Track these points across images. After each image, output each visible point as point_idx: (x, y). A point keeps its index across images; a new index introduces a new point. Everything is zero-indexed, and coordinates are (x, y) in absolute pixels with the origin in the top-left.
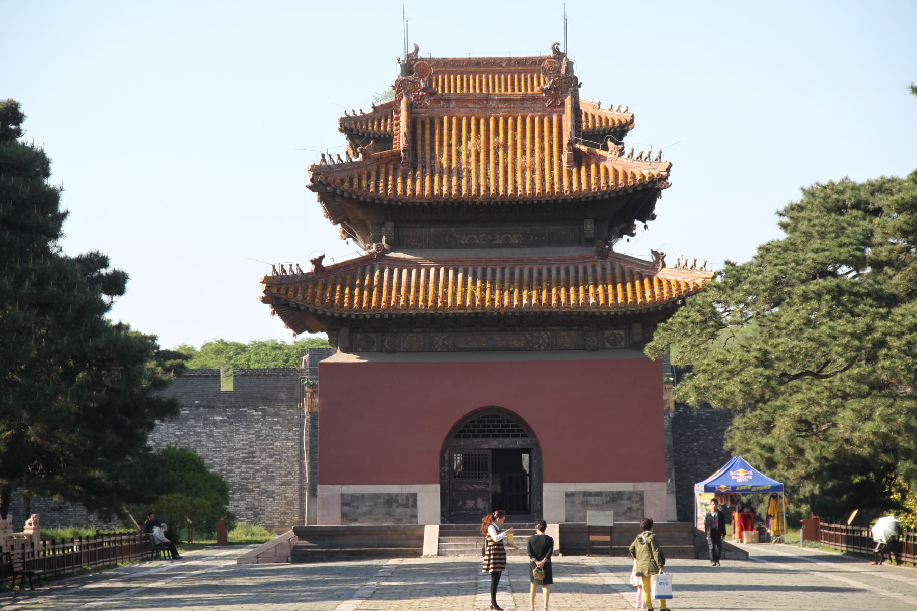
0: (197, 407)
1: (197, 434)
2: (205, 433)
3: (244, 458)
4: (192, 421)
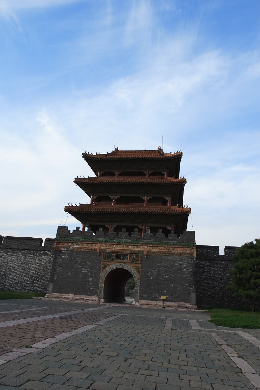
0: (32, 250)
1: (30, 259)
2: (33, 259)
3: (43, 268)
4: (29, 254)
